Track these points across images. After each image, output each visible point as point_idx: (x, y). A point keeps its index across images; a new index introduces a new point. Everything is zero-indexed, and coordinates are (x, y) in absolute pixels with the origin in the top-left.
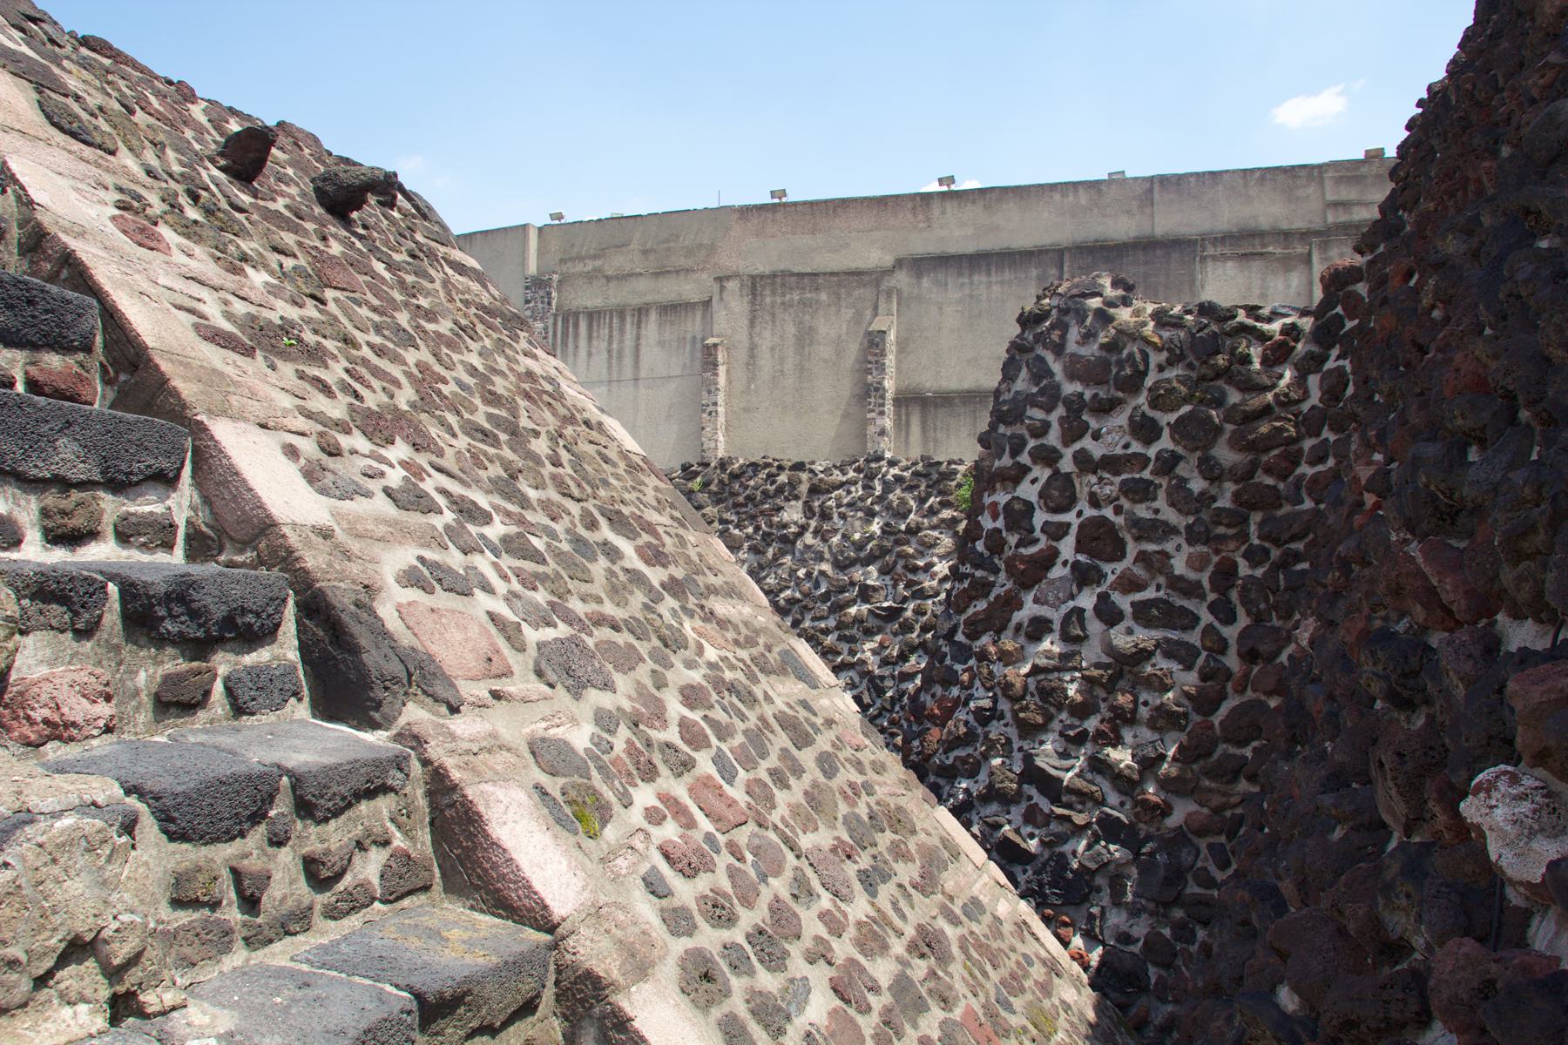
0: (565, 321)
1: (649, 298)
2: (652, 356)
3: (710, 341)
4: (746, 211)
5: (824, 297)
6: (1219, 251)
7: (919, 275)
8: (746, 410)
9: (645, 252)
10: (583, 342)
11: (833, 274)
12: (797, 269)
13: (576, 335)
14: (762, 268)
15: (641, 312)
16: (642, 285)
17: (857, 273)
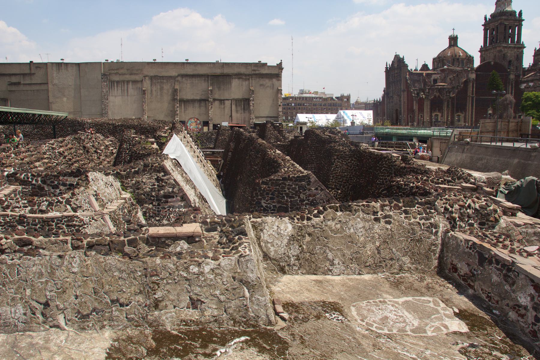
0: (111, 83)
1: (129, 79)
2: (131, 91)
3: (144, 89)
4: (149, 63)
5: (165, 81)
6: (235, 77)
7: (183, 78)
8: (151, 102)
9: (128, 70)
10: (116, 88)
11: (166, 77)
12: (159, 75)
13: (114, 86)
14: (152, 74)
15: (128, 82)
17: (171, 77)
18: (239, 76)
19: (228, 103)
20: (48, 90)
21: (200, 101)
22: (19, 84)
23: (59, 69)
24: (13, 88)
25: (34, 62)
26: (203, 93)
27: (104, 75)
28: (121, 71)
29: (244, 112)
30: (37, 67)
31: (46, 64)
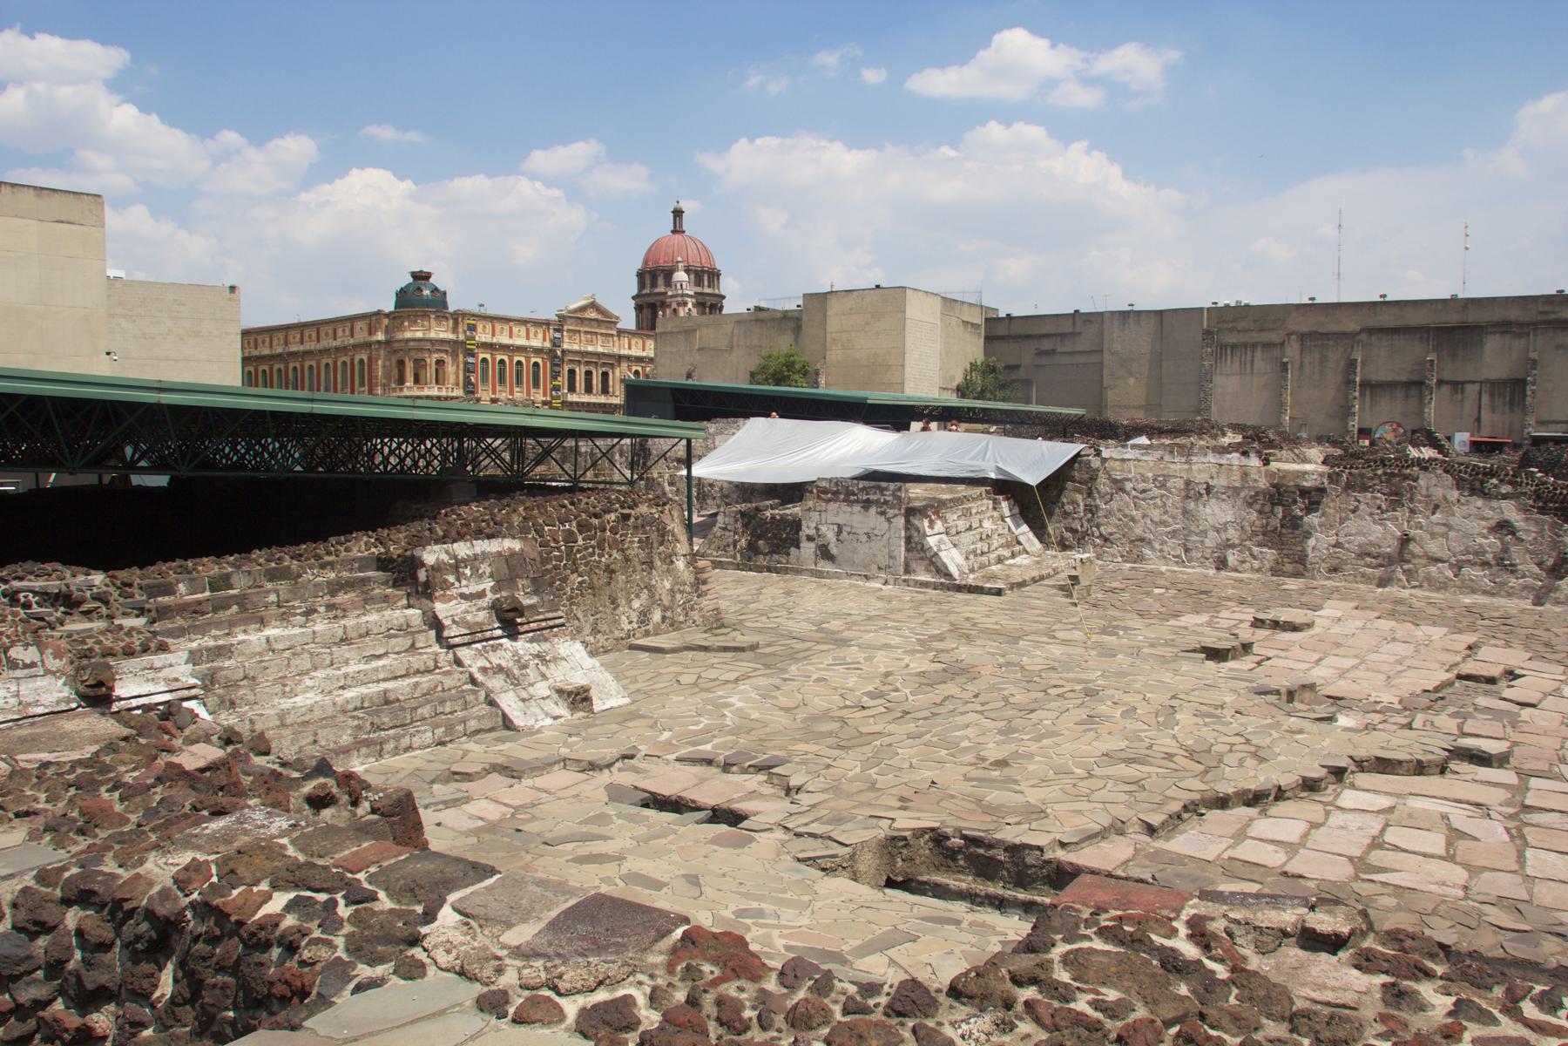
2: (1259, 364)
3: (1285, 360)
5: (1331, 343)
9: (1255, 321)
10: (1229, 357)
14: (1305, 329)
15: (1254, 346)
16: (1254, 334)
17: (1345, 335)
18: (1504, 327)
19: (1471, 390)
20: (1102, 363)
21: (1408, 385)
22: (1053, 352)
24: (1044, 361)
25: (1082, 311)
26: (1416, 367)
27: (1208, 333)
28: (1241, 325)
29: (1512, 411)
30: (1085, 321)
31: (1101, 314)
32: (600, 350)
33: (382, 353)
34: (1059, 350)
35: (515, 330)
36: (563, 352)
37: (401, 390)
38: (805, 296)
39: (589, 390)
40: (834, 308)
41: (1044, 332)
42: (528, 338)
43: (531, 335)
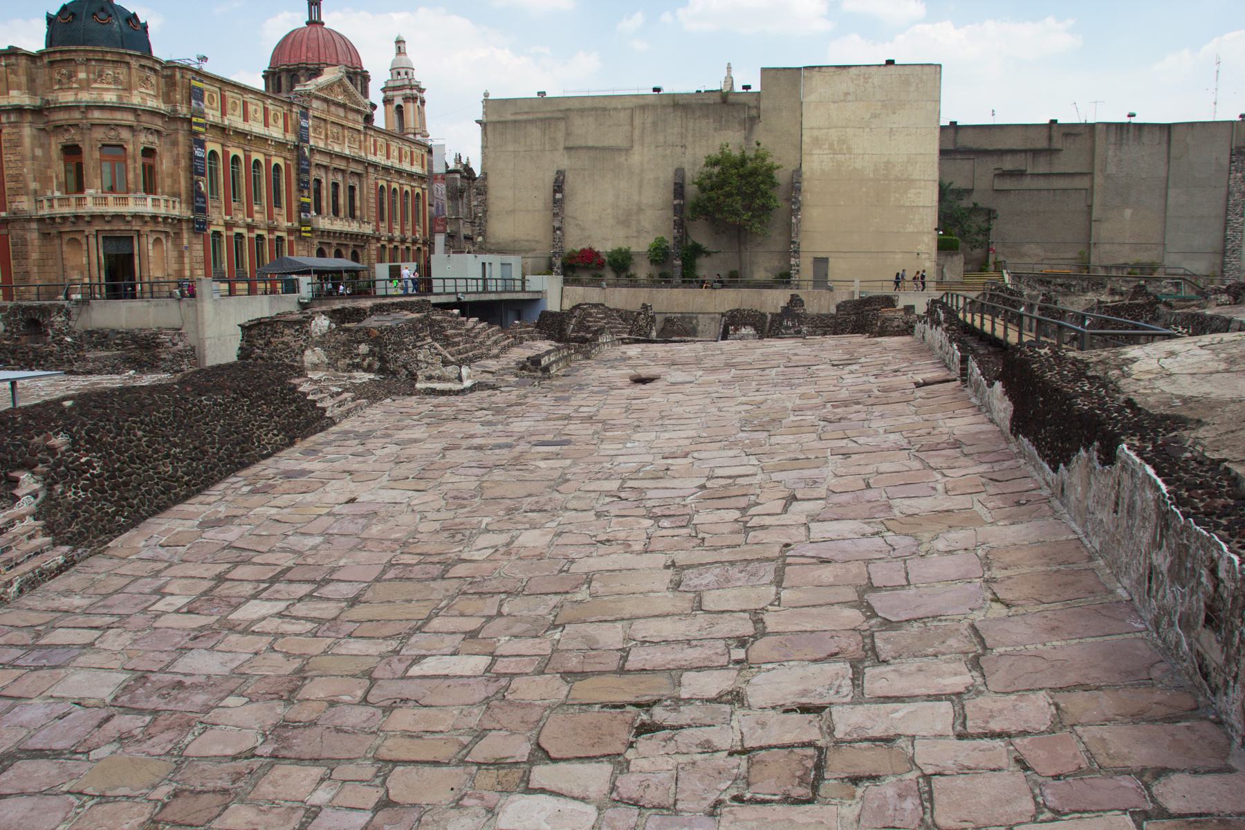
20: (1090, 191)
22: (1019, 174)
23: (1122, 139)
24: (1007, 184)
30: (1066, 135)
31: (1092, 127)
32: (347, 152)
33: (27, 131)
34: (1028, 172)
35: (251, 108)
36: (312, 150)
37: (80, 202)
38: (764, 71)
39: (336, 212)
40: (814, 93)
41: (1006, 147)
42: (266, 125)
43: (271, 121)
